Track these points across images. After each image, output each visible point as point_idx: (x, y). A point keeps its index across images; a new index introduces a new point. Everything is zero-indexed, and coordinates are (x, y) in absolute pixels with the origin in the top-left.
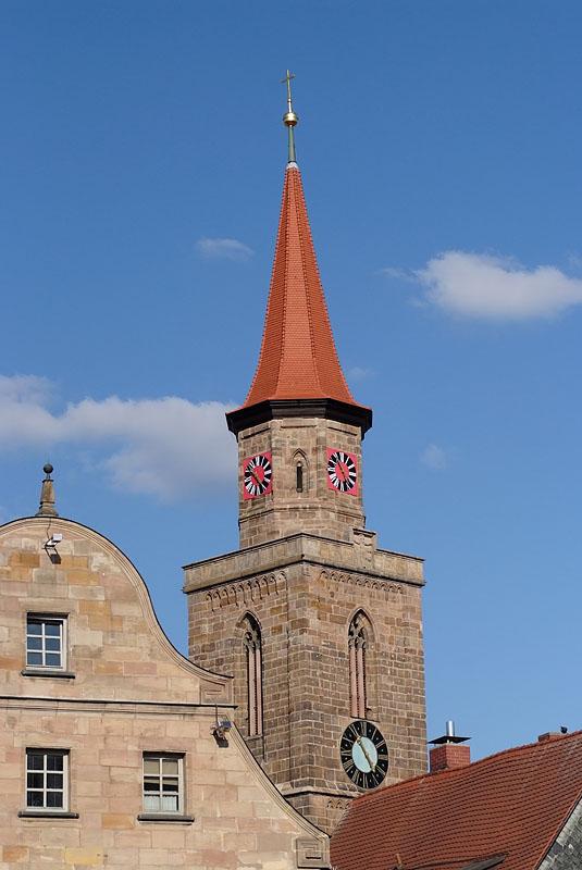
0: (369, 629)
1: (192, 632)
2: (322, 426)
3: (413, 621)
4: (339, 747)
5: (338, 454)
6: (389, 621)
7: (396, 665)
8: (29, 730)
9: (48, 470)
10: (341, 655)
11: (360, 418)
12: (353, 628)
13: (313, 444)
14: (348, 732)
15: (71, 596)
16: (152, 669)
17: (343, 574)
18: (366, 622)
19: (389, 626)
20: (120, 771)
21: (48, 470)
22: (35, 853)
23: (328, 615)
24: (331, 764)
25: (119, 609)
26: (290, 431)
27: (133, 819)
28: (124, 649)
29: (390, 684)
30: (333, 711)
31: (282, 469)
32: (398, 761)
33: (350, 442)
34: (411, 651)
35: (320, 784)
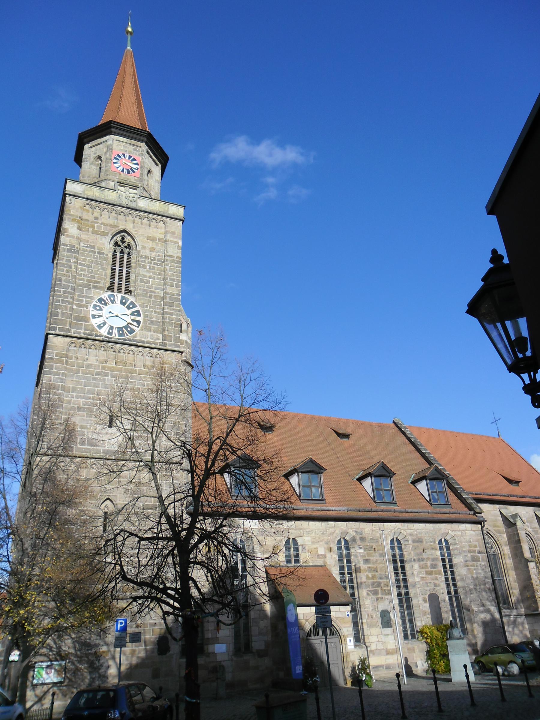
0: (133, 243)
3: (172, 239)
5: (124, 155)
7: (155, 264)
12: (120, 243)
13: (105, 150)
17: (106, 207)
18: (131, 240)
19: (151, 242)
23: (91, 229)
26: (93, 149)
29: (148, 275)
30: (88, 286)
32: (152, 322)
34: (170, 256)
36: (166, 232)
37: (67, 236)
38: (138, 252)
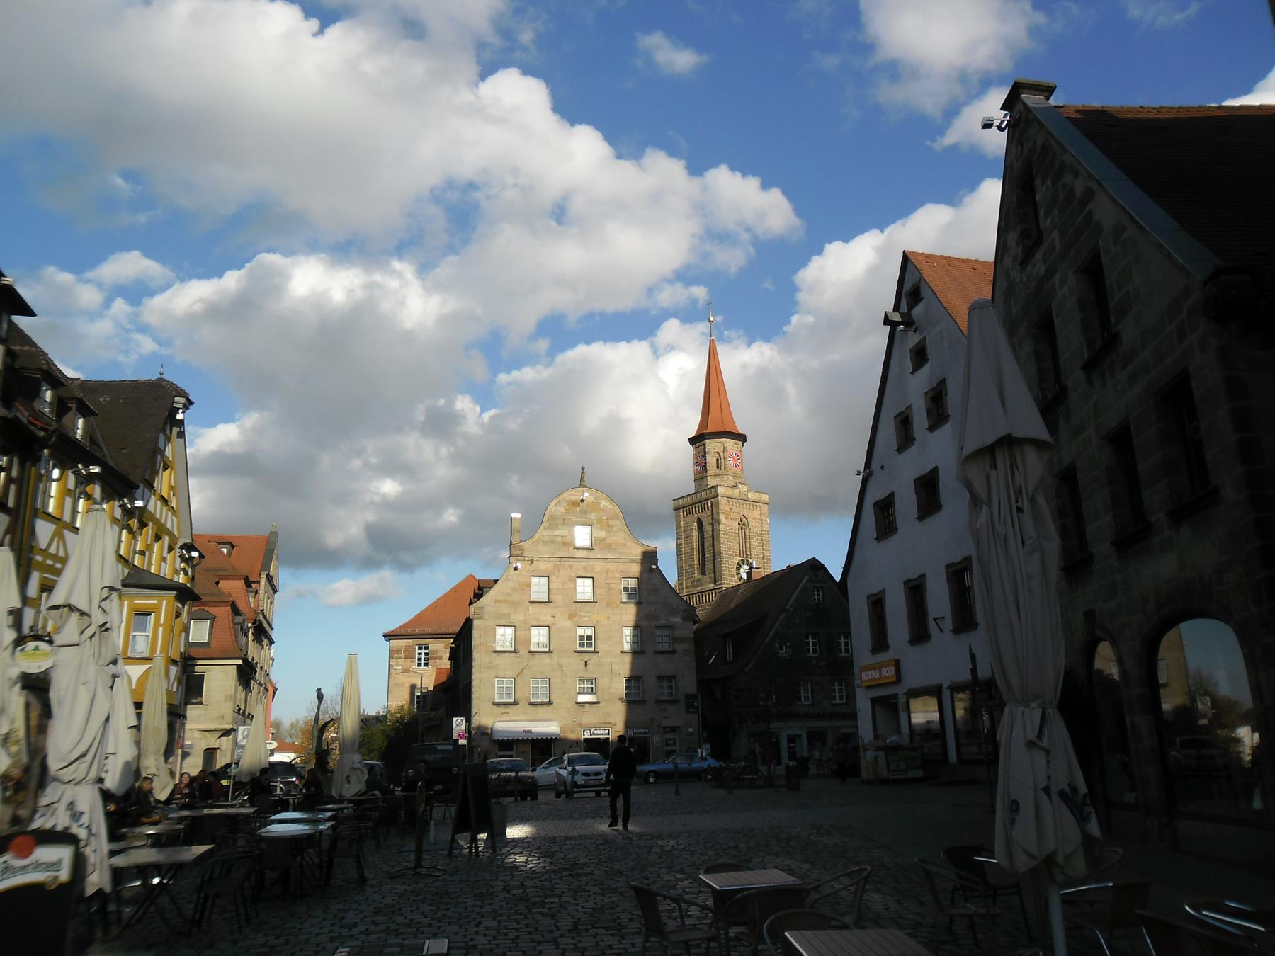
1: (677, 526)
2: (729, 443)
4: (735, 569)
6: (754, 519)
8: (577, 570)
9: (583, 469)
10: (735, 533)
11: (742, 438)
14: (738, 563)
15: (593, 518)
16: (624, 545)
20: (613, 585)
21: (583, 469)
22: (582, 617)
24: (733, 576)
25: (611, 522)
26: (713, 445)
27: (619, 603)
28: (615, 538)
30: (732, 555)
31: (711, 460)
33: (738, 448)
35: (727, 584)
36: (761, 514)
37: (723, 524)
38: (750, 529)
